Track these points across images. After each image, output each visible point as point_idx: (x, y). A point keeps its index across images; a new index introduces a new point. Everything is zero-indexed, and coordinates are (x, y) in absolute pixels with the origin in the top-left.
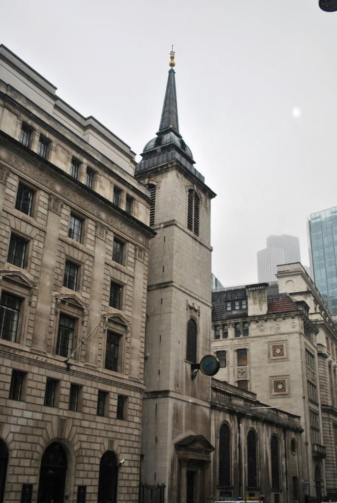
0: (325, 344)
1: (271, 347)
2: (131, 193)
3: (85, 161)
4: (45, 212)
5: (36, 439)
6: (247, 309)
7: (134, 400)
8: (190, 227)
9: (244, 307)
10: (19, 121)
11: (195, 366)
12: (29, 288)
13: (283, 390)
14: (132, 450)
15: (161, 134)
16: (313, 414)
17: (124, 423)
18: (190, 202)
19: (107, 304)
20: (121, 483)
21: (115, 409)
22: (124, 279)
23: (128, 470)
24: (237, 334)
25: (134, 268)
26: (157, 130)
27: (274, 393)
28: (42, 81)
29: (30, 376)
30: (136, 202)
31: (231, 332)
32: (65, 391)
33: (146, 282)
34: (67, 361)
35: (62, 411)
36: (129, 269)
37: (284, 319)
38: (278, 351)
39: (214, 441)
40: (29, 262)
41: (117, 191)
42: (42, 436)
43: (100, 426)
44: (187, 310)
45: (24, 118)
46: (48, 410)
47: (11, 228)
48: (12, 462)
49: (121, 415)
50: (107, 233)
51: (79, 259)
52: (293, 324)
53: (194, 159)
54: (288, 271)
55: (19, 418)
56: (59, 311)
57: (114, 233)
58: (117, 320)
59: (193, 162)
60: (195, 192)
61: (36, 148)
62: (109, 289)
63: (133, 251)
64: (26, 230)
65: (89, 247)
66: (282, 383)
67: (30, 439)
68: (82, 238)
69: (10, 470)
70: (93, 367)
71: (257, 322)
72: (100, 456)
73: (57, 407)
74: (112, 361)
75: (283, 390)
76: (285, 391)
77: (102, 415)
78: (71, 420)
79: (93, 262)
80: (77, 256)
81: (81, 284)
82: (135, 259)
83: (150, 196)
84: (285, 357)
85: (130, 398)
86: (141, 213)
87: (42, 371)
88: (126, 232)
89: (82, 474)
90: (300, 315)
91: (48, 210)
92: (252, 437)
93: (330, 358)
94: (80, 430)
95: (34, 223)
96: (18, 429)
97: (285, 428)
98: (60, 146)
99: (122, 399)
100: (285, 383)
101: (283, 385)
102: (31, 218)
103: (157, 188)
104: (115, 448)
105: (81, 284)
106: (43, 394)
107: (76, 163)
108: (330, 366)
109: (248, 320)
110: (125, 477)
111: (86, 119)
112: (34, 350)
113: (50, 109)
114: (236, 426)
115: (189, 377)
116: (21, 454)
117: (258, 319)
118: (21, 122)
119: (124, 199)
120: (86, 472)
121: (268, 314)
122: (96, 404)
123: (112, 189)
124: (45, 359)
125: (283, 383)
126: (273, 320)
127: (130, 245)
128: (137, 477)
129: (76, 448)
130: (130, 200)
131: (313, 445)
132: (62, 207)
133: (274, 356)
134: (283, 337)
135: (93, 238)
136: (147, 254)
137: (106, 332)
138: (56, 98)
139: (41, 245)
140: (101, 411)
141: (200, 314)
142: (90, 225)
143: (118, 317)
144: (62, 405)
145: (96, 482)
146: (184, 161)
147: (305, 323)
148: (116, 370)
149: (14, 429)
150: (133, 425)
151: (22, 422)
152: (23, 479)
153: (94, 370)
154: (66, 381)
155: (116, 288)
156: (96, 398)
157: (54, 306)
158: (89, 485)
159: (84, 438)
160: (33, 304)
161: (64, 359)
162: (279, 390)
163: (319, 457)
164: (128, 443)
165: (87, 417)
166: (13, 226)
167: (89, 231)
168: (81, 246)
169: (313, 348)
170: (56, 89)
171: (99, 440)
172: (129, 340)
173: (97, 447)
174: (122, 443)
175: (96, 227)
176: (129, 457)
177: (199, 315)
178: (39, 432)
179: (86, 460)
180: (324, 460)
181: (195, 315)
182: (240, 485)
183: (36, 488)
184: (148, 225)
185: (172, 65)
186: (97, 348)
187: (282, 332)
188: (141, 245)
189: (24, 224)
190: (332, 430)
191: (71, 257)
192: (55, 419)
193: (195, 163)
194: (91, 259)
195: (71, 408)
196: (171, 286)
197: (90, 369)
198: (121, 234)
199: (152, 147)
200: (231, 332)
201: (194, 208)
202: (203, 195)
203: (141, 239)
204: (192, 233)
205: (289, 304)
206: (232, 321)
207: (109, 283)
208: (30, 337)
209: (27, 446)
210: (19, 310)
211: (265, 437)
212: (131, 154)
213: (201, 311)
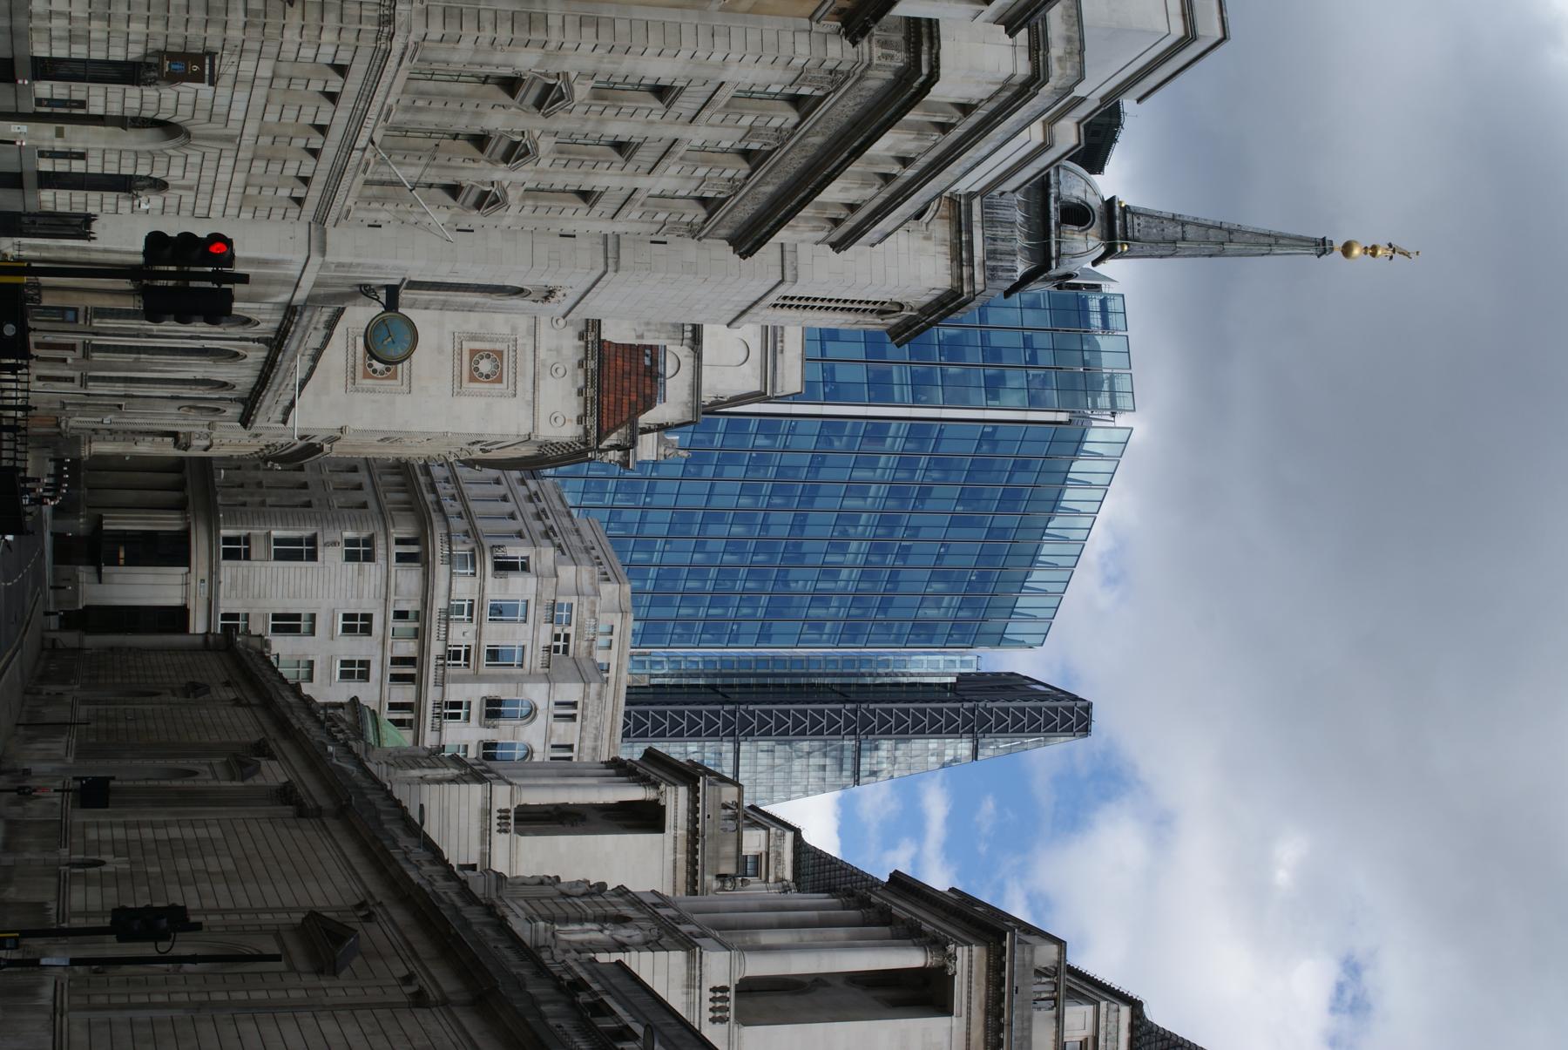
1: (498, 346)
11: (393, 292)
13: (370, 370)
28: (1153, 85)
34: (373, 143)
37: (580, 392)
38: (485, 366)
52: (560, 421)
54: (782, 352)
60: (895, 312)
75: (370, 370)
81: (571, 157)
84: (465, 383)
90: (586, 443)
100: (387, 378)
105: (571, 157)
121: (601, 342)
126: (581, 355)
133: (473, 352)
134: (525, 384)
170: (1139, 100)
182: (96, 334)
187: (542, 384)
192: (234, 129)
204: (772, 299)
205: (625, 409)
213: (547, 305)
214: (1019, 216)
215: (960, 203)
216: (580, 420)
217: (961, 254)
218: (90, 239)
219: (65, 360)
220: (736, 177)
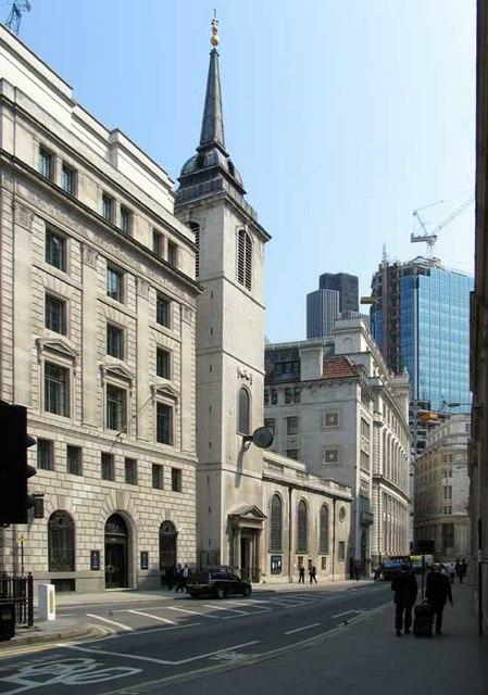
2: (173, 238)
5: (97, 511)
7: (188, 473)
14: (188, 520)
21: (170, 482)
22: (170, 344)
23: (186, 537)
32: (120, 465)
43: (157, 498)
48: (78, 531)
49: (176, 487)
51: (121, 323)
58: (167, 392)
59: (242, 192)
62: (155, 356)
67: (92, 510)
69: (77, 538)
72: (159, 525)
74: (164, 434)
83: (194, 241)
87: (96, 446)
88: (170, 288)
89: (143, 541)
94: (138, 502)
96: (79, 502)
99: (176, 473)
103: (201, 227)
104: (172, 518)
116: (85, 524)
140: (157, 483)
143: (168, 388)
145: (157, 548)
146: (232, 192)
149: (75, 501)
150: (187, 497)
151: (82, 494)
152: (92, 547)
154: (120, 455)
155: (163, 356)
156: (150, 472)
159: (142, 509)
164: (185, 514)
165: (143, 489)
169: (369, 417)
173: (154, 517)
174: (179, 513)
176: (186, 525)
178: (99, 504)
183: (103, 554)
184: (194, 278)
186: (148, 421)
192: (113, 493)
209: (91, 517)
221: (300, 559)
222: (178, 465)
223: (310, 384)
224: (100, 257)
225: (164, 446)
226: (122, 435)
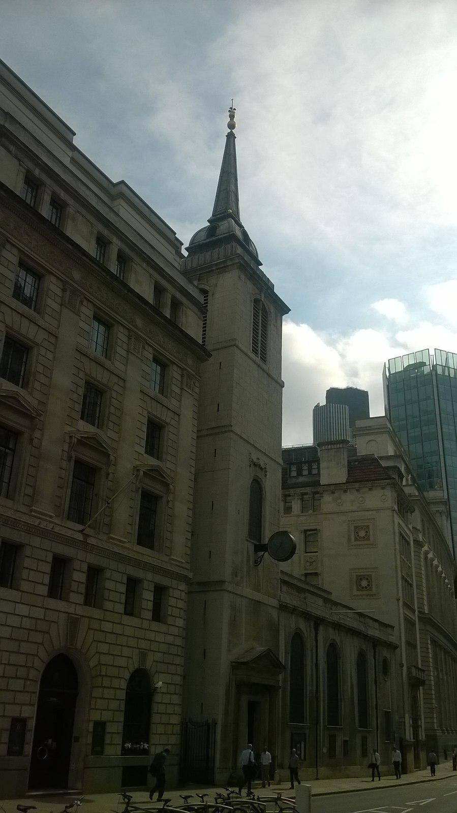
0: (421, 530)
1: (353, 529)
2: (178, 295)
3: (115, 240)
4: (57, 307)
6: (319, 474)
8: (255, 351)
9: (315, 472)
10: (21, 168)
11: (260, 548)
12: (31, 418)
13: (368, 588)
15: (214, 221)
16: (410, 623)
17: (163, 628)
18: (256, 316)
19: (142, 451)
20: (155, 718)
21: (150, 606)
22: (166, 416)
23: (166, 698)
24: (303, 509)
25: (180, 401)
26: (209, 215)
27: (355, 593)
29: (28, 551)
30: (184, 308)
31: (296, 506)
33: (196, 422)
34: (83, 530)
35: (73, 605)
36: (173, 403)
37: (370, 489)
38: (362, 534)
39: (283, 657)
40: (32, 379)
41: (159, 291)
42: (42, 644)
44: (250, 466)
45: (29, 164)
46: (53, 603)
47: (7, 326)
49: (157, 615)
50: (144, 348)
53: (260, 259)
55: (9, 616)
56: (74, 454)
57: (154, 349)
58: (155, 474)
60: (263, 303)
61: (46, 211)
62: (145, 429)
63: (179, 378)
64: (28, 331)
65: (118, 366)
66: (367, 579)
68: (108, 349)
70: (121, 541)
71: (333, 493)
72: (127, 676)
73: (67, 600)
75: (368, 588)
76: (371, 590)
77: (131, 614)
78: (87, 619)
79: (124, 388)
80: (101, 376)
82: (182, 389)
85: (171, 590)
86: (191, 324)
91: (61, 305)
92: (334, 653)
93: (426, 548)
95: (41, 322)
97: (375, 643)
98: (80, 213)
99: (160, 591)
101: (369, 582)
102: (35, 314)
103: (210, 294)
106: (47, 580)
107: (102, 243)
108: (426, 558)
109: (320, 489)
110: (162, 708)
111: (114, 185)
112: (35, 511)
113: (67, 161)
114: (313, 635)
115: (251, 563)
117: (334, 488)
118: (25, 171)
119: (169, 302)
120: (107, 701)
121: (347, 482)
122: (123, 596)
123: (153, 287)
124: (51, 526)
125: (368, 578)
127: (175, 368)
128: (178, 709)
129: (92, 664)
130: (176, 305)
131: (409, 668)
132: (81, 302)
133: (356, 540)
135: (124, 353)
136: (197, 384)
137: (140, 490)
138: (74, 148)
139: (50, 356)
140: (130, 609)
141: (267, 473)
142: (121, 335)
144: (73, 597)
145: (121, 717)
147: (398, 496)
148: (152, 548)
151: (14, 621)
153: (122, 546)
154: (81, 561)
155: (155, 429)
157: (66, 447)
158: (110, 721)
159: (104, 648)
160: (36, 441)
161: (81, 527)
162: (363, 588)
163: (416, 683)
166: (9, 322)
167: (119, 342)
168: (107, 363)
170: (74, 134)
171: (126, 652)
172: (170, 504)
173: (122, 662)
174: (158, 656)
175: (129, 338)
177: (266, 476)
179: (106, 682)
180: (421, 688)
181: (260, 474)
185: (232, 126)
188: (190, 370)
189: (25, 322)
190: (430, 646)
191: (92, 378)
193: (262, 265)
194: (121, 383)
195: (87, 603)
196: (229, 431)
197: (115, 544)
198: (161, 350)
199: (203, 239)
200: (296, 506)
201: (260, 325)
202: (272, 309)
203: (190, 362)
204: (258, 360)
206: (299, 491)
207: (145, 421)
208: (29, 491)
210: (14, 451)
211: (350, 650)
212: (176, 242)
213: (268, 470)
214: (209, 253)
215: (200, 274)
216: (383, 488)
217: (222, 267)
218: (215, 724)
219: (345, 742)
220: (61, 287)
221: (332, 739)
222: (165, 581)
223: (332, 488)
224: (85, 303)
225: (146, 551)
226: (89, 531)
